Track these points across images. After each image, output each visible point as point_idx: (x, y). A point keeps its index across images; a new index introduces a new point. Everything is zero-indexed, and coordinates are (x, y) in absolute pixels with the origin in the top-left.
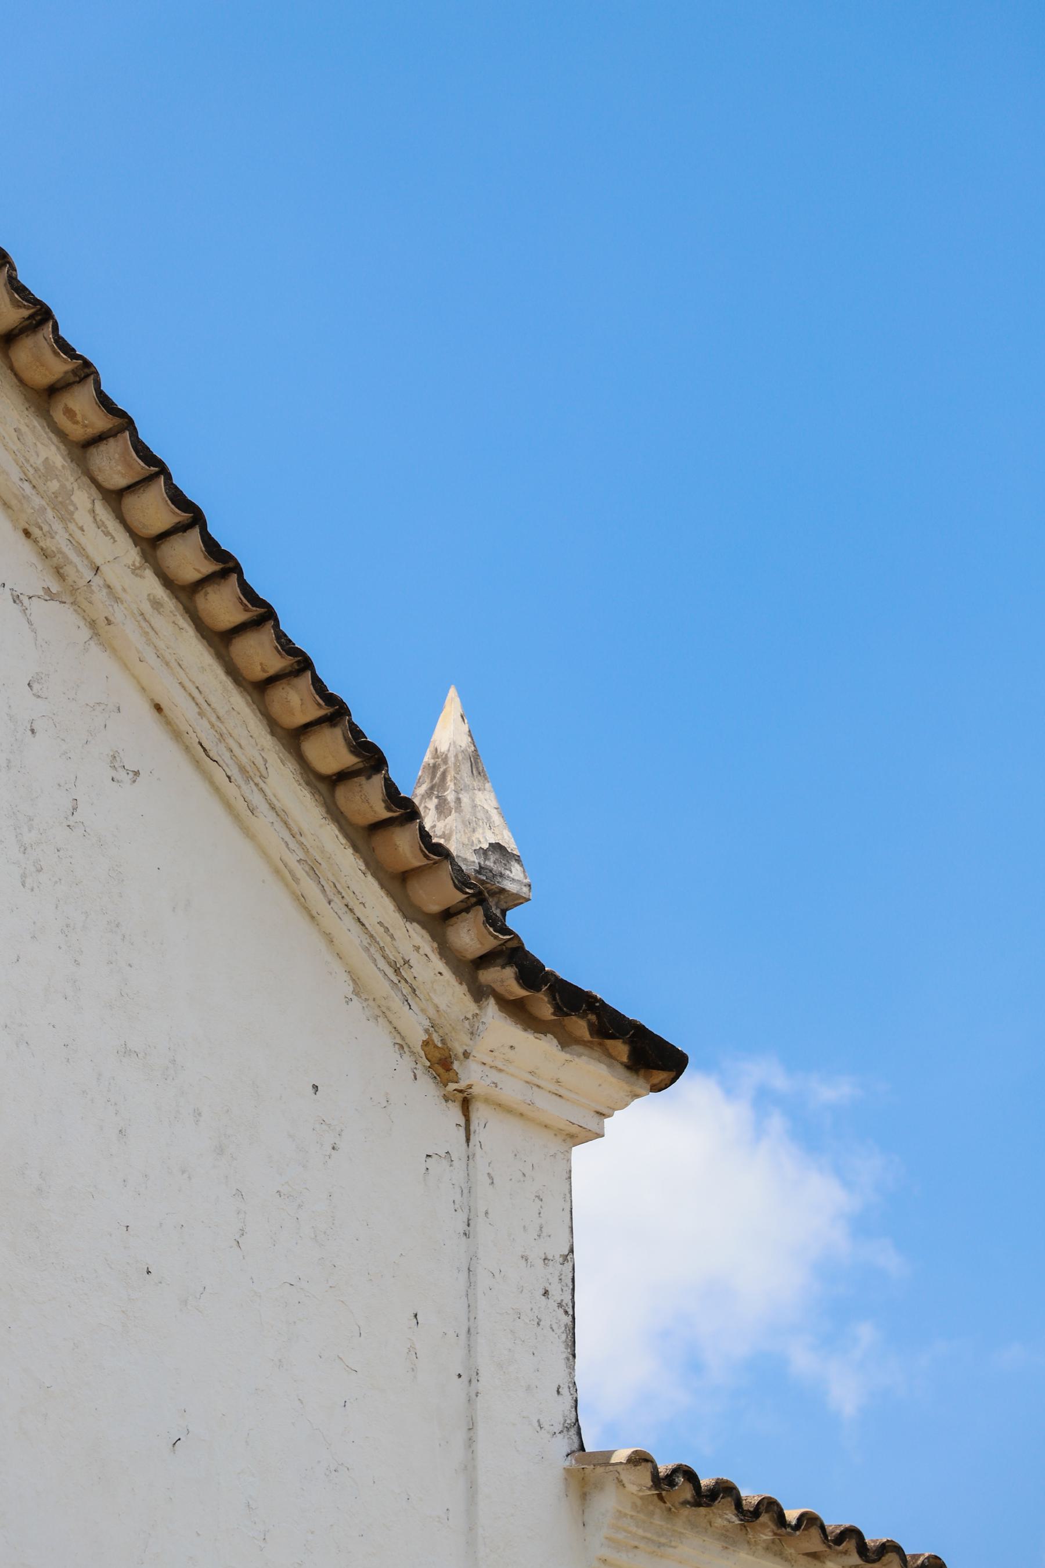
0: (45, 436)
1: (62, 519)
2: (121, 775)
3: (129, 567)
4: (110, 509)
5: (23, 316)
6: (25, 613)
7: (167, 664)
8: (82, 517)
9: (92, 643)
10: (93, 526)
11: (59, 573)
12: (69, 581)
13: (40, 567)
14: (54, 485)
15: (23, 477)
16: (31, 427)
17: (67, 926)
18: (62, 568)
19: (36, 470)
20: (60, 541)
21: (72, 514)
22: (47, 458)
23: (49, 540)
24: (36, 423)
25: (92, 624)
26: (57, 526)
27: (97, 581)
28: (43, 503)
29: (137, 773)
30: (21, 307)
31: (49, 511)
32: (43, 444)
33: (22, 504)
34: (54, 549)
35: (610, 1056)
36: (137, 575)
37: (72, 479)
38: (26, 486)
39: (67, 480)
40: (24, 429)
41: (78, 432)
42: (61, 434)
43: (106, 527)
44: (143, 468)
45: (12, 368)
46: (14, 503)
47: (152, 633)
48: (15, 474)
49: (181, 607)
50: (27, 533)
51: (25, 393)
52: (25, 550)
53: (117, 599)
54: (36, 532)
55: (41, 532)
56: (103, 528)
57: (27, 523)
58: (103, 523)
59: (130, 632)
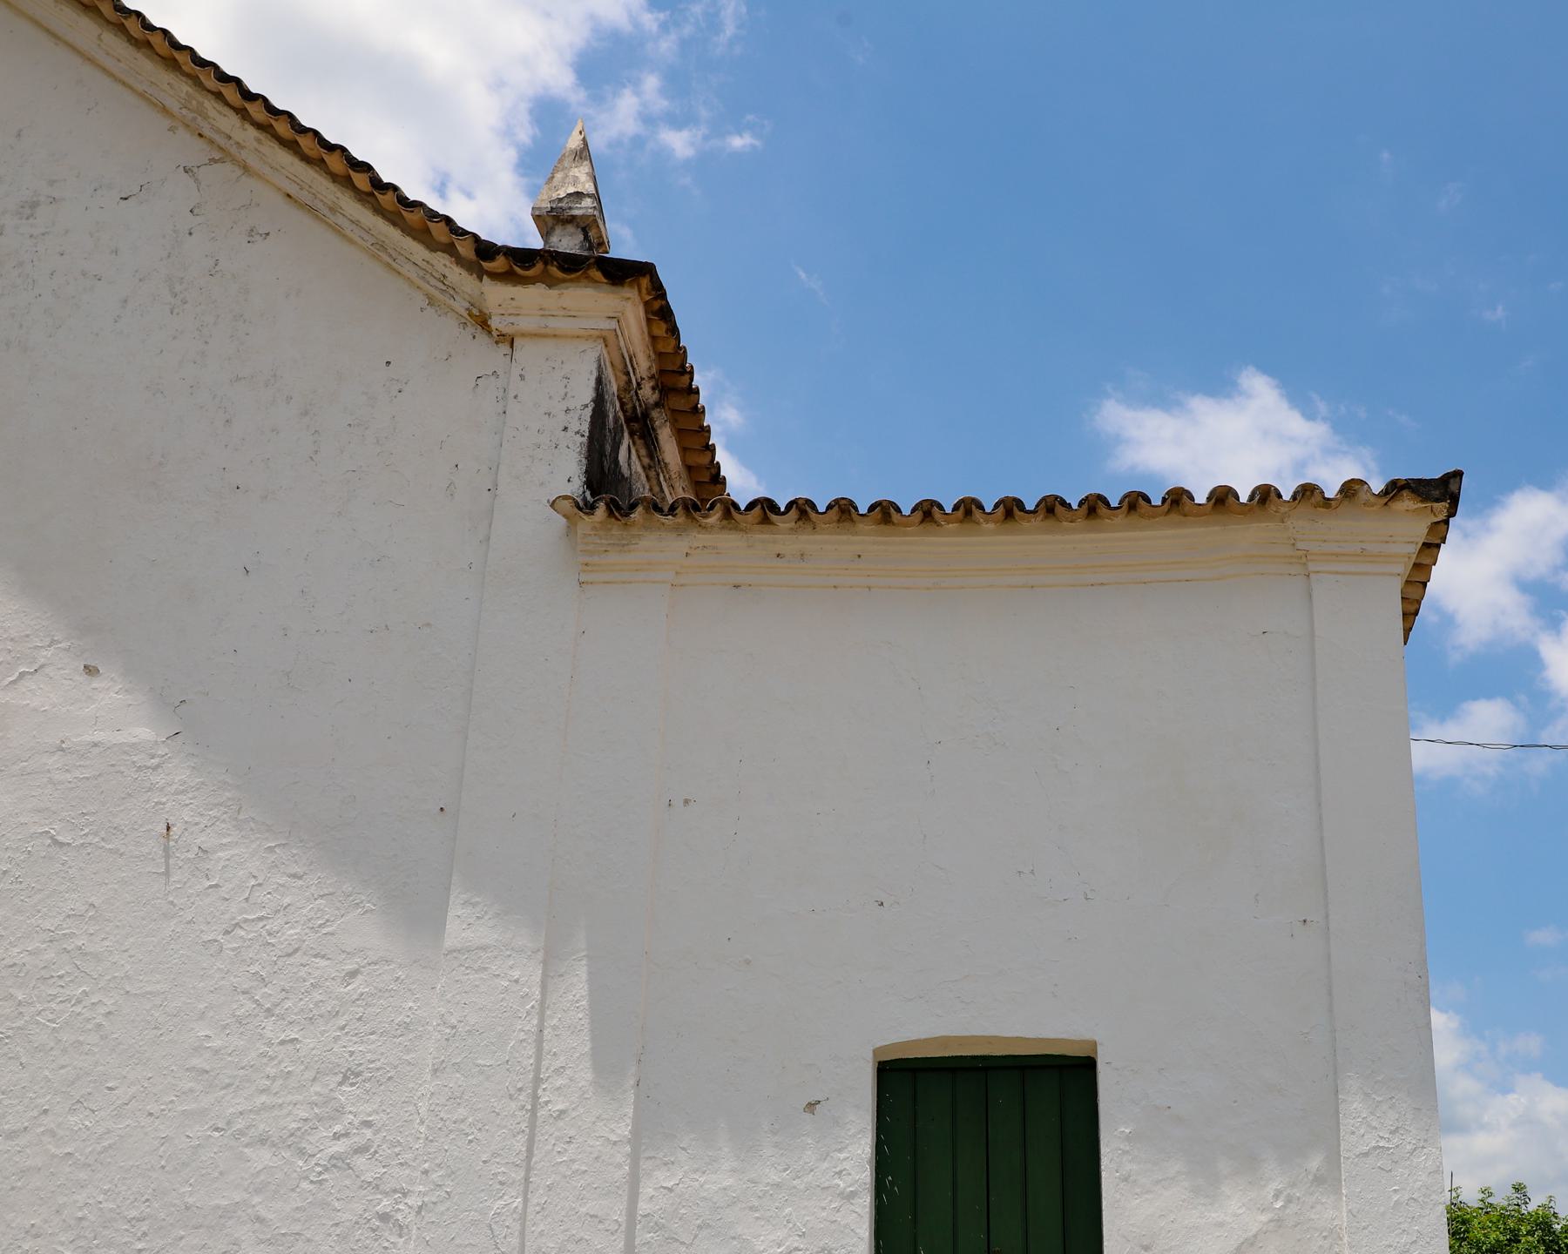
7: (276, 169)
27: (232, 142)
31: (199, 117)
35: (596, 282)
40: (171, 81)
49: (269, 136)
53: (243, 148)
59: (253, 161)
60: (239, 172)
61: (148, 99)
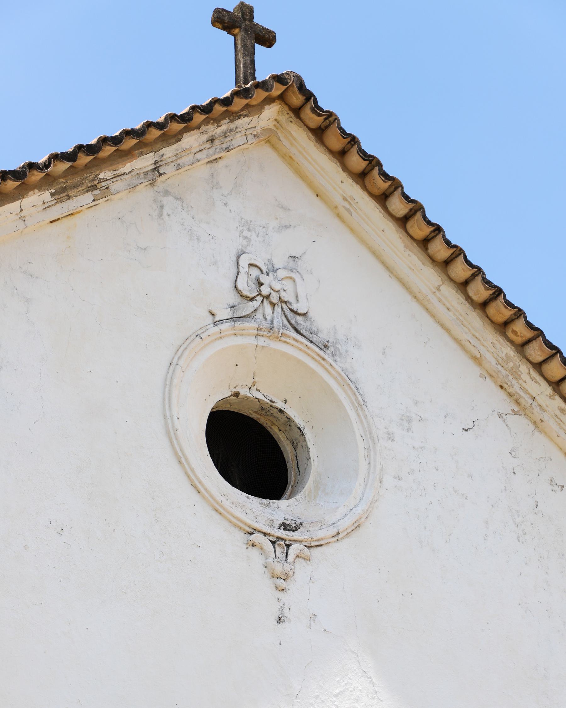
0: (505, 343)
1: (516, 379)
2: (556, 488)
3: (548, 396)
4: (536, 371)
6: (505, 422)
8: (525, 377)
9: (535, 431)
10: (530, 380)
11: (517, 402)
12: (522, 405)
13: (509, 401)
14: (511, 364)
15: (497, 363)
17: (541, 557)
18: (518, 400)
19: (502, 359)
20: (516, 389)
21: (520, 376)
22: (507, 353)
23: (511, 388)
24: (501, 339)
25: (535, 423)
26: (514, 382)
27: (534, 404)
28: (507, 373)
29: (563, 486)
31: (510, 375)
32: (504, 347)
33: (498, 374)
34: (514, 392)
36: (552, 399)
37: (518, 361)
39: (516, 361)
40: (495, 342)
41: (519, 340)
42: (512, 342)
43: (536, 380)
44: (549, 352)
45: (487, 317)
46: (494, 374)
47: (562, 424)
48: (494, 362)
50: (501, 387)
51: (494, 326)
52: (502, 394)
53: (544, 411)
54: (505, 386)
55: (507, 386)
56: (534, 380)
58: (534, 378)
59: (551, 424)
60: (532, 427)
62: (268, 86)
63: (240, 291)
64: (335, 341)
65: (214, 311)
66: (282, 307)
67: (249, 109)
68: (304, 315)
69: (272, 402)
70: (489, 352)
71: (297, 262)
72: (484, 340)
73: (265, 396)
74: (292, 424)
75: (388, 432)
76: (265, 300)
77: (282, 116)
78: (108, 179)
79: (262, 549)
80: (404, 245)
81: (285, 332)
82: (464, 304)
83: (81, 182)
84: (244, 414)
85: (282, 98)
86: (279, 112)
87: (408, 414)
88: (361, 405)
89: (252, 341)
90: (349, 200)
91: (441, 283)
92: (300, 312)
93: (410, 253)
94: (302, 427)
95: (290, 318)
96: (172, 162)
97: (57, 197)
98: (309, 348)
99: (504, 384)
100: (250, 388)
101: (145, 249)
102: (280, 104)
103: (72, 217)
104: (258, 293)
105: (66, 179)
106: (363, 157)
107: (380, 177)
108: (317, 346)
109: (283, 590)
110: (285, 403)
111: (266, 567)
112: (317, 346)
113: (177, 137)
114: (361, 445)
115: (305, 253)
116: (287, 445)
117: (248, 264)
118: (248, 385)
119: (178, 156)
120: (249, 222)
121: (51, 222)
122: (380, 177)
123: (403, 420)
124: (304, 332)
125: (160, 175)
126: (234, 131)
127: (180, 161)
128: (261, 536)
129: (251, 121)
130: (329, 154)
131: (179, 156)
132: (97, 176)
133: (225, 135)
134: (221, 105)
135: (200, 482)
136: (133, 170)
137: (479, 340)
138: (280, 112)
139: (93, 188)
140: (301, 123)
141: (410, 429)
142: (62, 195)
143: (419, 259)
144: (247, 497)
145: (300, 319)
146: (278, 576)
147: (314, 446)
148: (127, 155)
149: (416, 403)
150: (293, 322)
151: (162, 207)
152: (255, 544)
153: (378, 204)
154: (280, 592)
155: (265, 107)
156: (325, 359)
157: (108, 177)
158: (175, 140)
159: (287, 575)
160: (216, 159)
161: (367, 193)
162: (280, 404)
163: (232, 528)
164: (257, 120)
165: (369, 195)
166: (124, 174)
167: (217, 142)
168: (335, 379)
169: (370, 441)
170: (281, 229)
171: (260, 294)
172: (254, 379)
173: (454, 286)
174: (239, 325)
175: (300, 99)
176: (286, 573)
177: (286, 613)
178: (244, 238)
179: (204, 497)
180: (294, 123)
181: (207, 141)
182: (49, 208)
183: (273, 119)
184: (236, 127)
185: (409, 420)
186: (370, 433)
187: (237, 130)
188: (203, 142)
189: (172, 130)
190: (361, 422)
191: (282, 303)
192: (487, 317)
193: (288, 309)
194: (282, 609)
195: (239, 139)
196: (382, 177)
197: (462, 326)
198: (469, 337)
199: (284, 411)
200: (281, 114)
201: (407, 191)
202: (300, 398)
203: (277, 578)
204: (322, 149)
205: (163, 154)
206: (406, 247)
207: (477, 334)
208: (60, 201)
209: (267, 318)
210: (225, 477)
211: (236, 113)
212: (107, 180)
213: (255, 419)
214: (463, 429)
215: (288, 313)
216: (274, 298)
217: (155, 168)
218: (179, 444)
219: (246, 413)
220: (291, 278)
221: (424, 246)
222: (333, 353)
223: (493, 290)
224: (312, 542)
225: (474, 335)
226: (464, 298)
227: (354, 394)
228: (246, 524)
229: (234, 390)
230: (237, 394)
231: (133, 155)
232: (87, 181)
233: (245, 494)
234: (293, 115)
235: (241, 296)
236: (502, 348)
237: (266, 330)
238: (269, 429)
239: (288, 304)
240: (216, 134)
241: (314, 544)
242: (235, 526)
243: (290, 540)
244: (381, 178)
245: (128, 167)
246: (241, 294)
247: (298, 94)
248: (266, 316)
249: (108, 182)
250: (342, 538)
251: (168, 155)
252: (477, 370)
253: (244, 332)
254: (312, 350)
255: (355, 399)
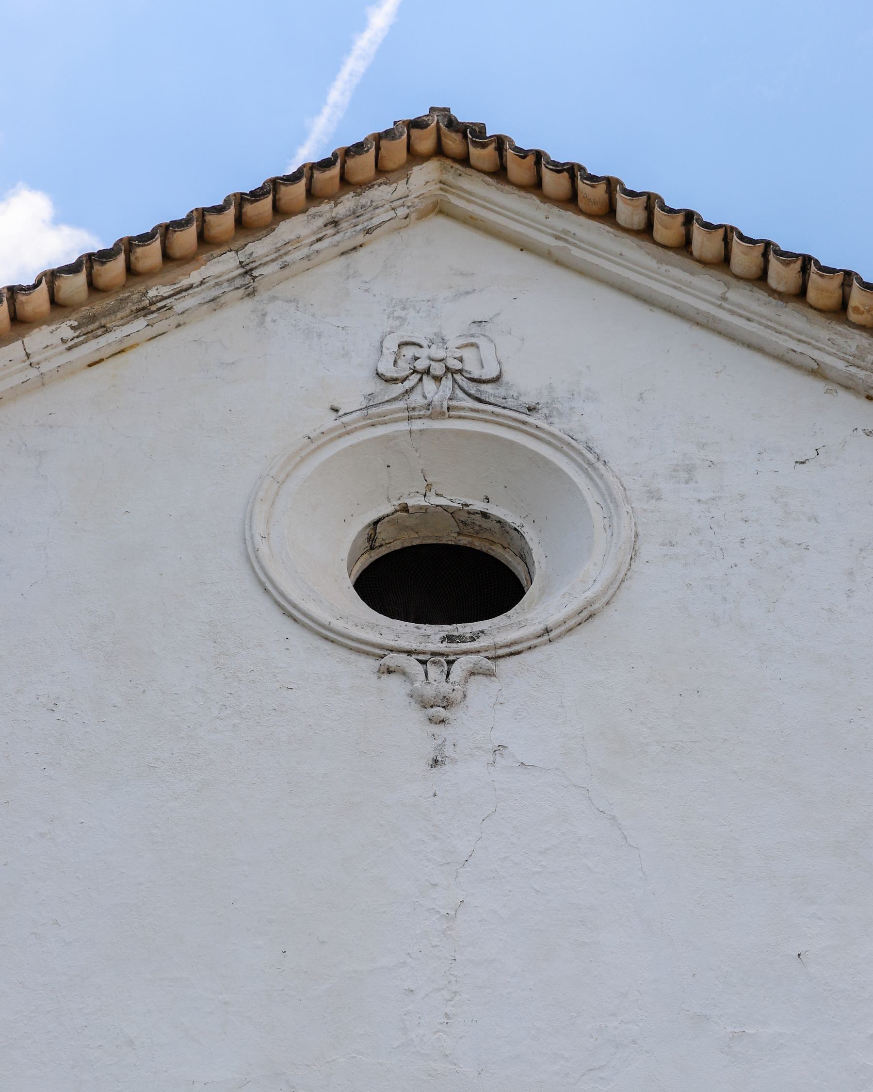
0: (849, 332)
5: (797, 271)
15: (846, 364)
16: (838, 333)
19: (854, 356)
24: (840, 328)
30: (789, 263)
33: (854, 381)
38: (853, 370)
45: (811, 307)
51: (826, 316)
57: (865, 391)
61: (789, 363)
62: (394, 133)
63: (382, 374)
64: (550, 401)
65: (336, 405)
66: (454, 381)
67: (388, 176)
68: (496, 380)
69: (467, 505)
70: (830, 355)
71: (484, 326)
72: (816, 341)
73: (453, 500)
74: (508, 529)
75: (649, 490)
76: (425, 377)
77: (446, 174)
78: (164, 295)
79: (404, 673)
80: (656, 261)
81: (454, 403)
82: (768, 303)
83: (120, 306)
84: (450, 543)
85: (439, 151)
86: (441, 171)
87: (688, 462)
88: (593, 464)
89: (404, 426)
90: (563, 236)
91: (727, 289)
92: (484, 378)
93: (668, 268)
94: (518, 526)
95: (466, 389)
96: (273, 260)
97: (84, 330)
98: (498, 415)
99: (870, 391)
100: (425, 496)
101: (233, 363)
102: (438, 161)
103: (123, 354)
104: (412, 371)
105: (91, 305)
106: (554, 168)
107: (584, 183)
108: (515, 410)
109: (443, 721)
110: (488, 502)
111: (412, 697)
112: (515, 410)
113: (268, 228)
114: (597, 514)
115: (498, 314)
116: (519, 564)
117: (398, 342)
118: (419, 491)
119: (280, 252)
120: (404, 300)
121: (90, 366)
122: (584, 183)
123: (677, 471)
124: (492, 400)
125: (254, 278)
126: (370, 206)
127: (285, 258)
128: (405, 655)
129: (396, 189)
130: (519, 191)
131: (282, 252)
132: (145, 294)
133: (355, 214)
134: (319, 170)
135: (295, 607)
136: (204, 279)
137: (809, 344)
138: (444, 169)
139: (143, 311)
140: (473, 170)
141: (692, 479)
142: (90, 326)
143: (684, 271)
144: (416, 627)
145: (484, 387)
146: (432, 703)
147: (540, 545)
148: (188, 260)
149: (703, 446)
150: (473, 392)
151: (264, 315)
152: (391, 669)
153: (603, 224)
154: (438, 725)
155: (414, 168)
156: (526, 423)
157: (164, 293)
158: (266, 232)
159: (447, 699)
160: (355, 249)
161: (584, 216)
162: (478, 505)
163: (354, 657)
164: (405, 186)
165: (588, 218)
166: (191, 287)
167: (344, 225)
168: (549, 443)
169: (611, 505)
170: (459, 297)
171: (415, 371)
172: (426, 480)
173: (746, 284)
174: (374, 410)
175: (456, 140)
176: (444, 697)
177: (449, 751)
178: (395, 319)
179: (304, 626)
180: (464, 175)
181: (325, 226)
182: (77, 348)
183: (436, 181)
184: (372, 201)
185: (690, 469)
186: (611, 495)
187: (374, 204)
188: (318, 227)
189: (254, 219)
190: (596, 485)
191: (454, 375)
192: (811, 307)
193: (465, 379)
194: (441, 748)
195: (382, 216)
196: (586, 182)
197: (778, 334)
198: (793, 345)
199: (487, 513)
200: (444, 172)
201: (628, 187)
202: (506, 487)
203: (432, 707)
204: (508, 188)
205: (253, 252)
206: (660, 261)
207: (803, 338)
208: (91, 335)
209: (427, 395)
210: (393, 617)
211: (365, 184)
212: (166, 298)
213: (469, 546)
214: (796, 462)
215: (472, 388)
216: (438, 369)
217: (246, 273)
218: (262, 568)
219: (451, 541)
220: (472, 345)
221: (688, 252)
222: (547, 415)
223: (797, 260)
224: (497, 650)
225: (800, 340)
226: (767, 294)
227: (580, 453)
228: (374, 645)
229: (397, 503)
230: (405, 508)
231: (198, 260)
232: (130, 304)
233: (411, 625)
234: (460, 166)
235: (386, 381)
236: (848, 340)
237: (422, 409)
238: (492, 554)
239: (464, 374)
240: (338, 215)
241: (501, 652)
242: (359, 651)
243: (455, 654)
244: (586, 183)
245: (195, 277)
246: (385, 379)
247: (449, 133)
248: (426, 394)
249: (168, 301)
250: (560, 636)
251: (259, 253)
252: (820, 386)
253: (385, 418)
254: (504, 416)
255: (583, 459)
